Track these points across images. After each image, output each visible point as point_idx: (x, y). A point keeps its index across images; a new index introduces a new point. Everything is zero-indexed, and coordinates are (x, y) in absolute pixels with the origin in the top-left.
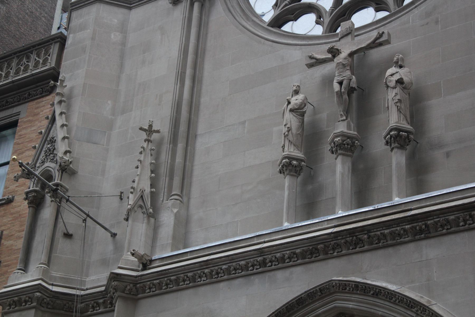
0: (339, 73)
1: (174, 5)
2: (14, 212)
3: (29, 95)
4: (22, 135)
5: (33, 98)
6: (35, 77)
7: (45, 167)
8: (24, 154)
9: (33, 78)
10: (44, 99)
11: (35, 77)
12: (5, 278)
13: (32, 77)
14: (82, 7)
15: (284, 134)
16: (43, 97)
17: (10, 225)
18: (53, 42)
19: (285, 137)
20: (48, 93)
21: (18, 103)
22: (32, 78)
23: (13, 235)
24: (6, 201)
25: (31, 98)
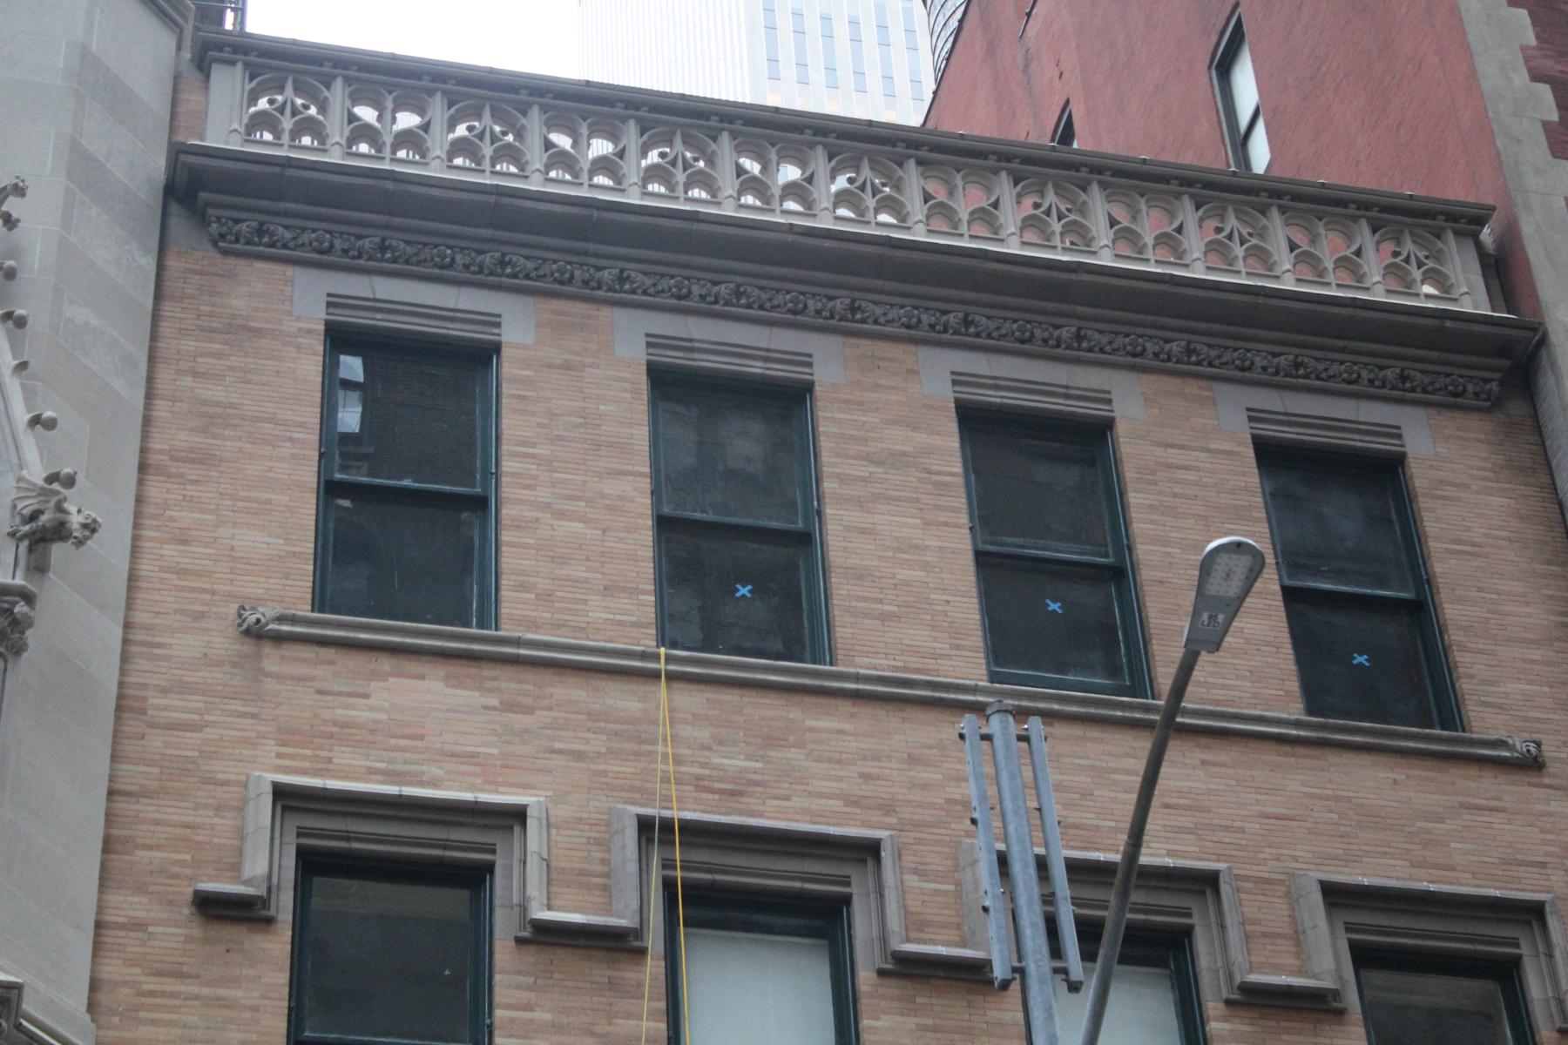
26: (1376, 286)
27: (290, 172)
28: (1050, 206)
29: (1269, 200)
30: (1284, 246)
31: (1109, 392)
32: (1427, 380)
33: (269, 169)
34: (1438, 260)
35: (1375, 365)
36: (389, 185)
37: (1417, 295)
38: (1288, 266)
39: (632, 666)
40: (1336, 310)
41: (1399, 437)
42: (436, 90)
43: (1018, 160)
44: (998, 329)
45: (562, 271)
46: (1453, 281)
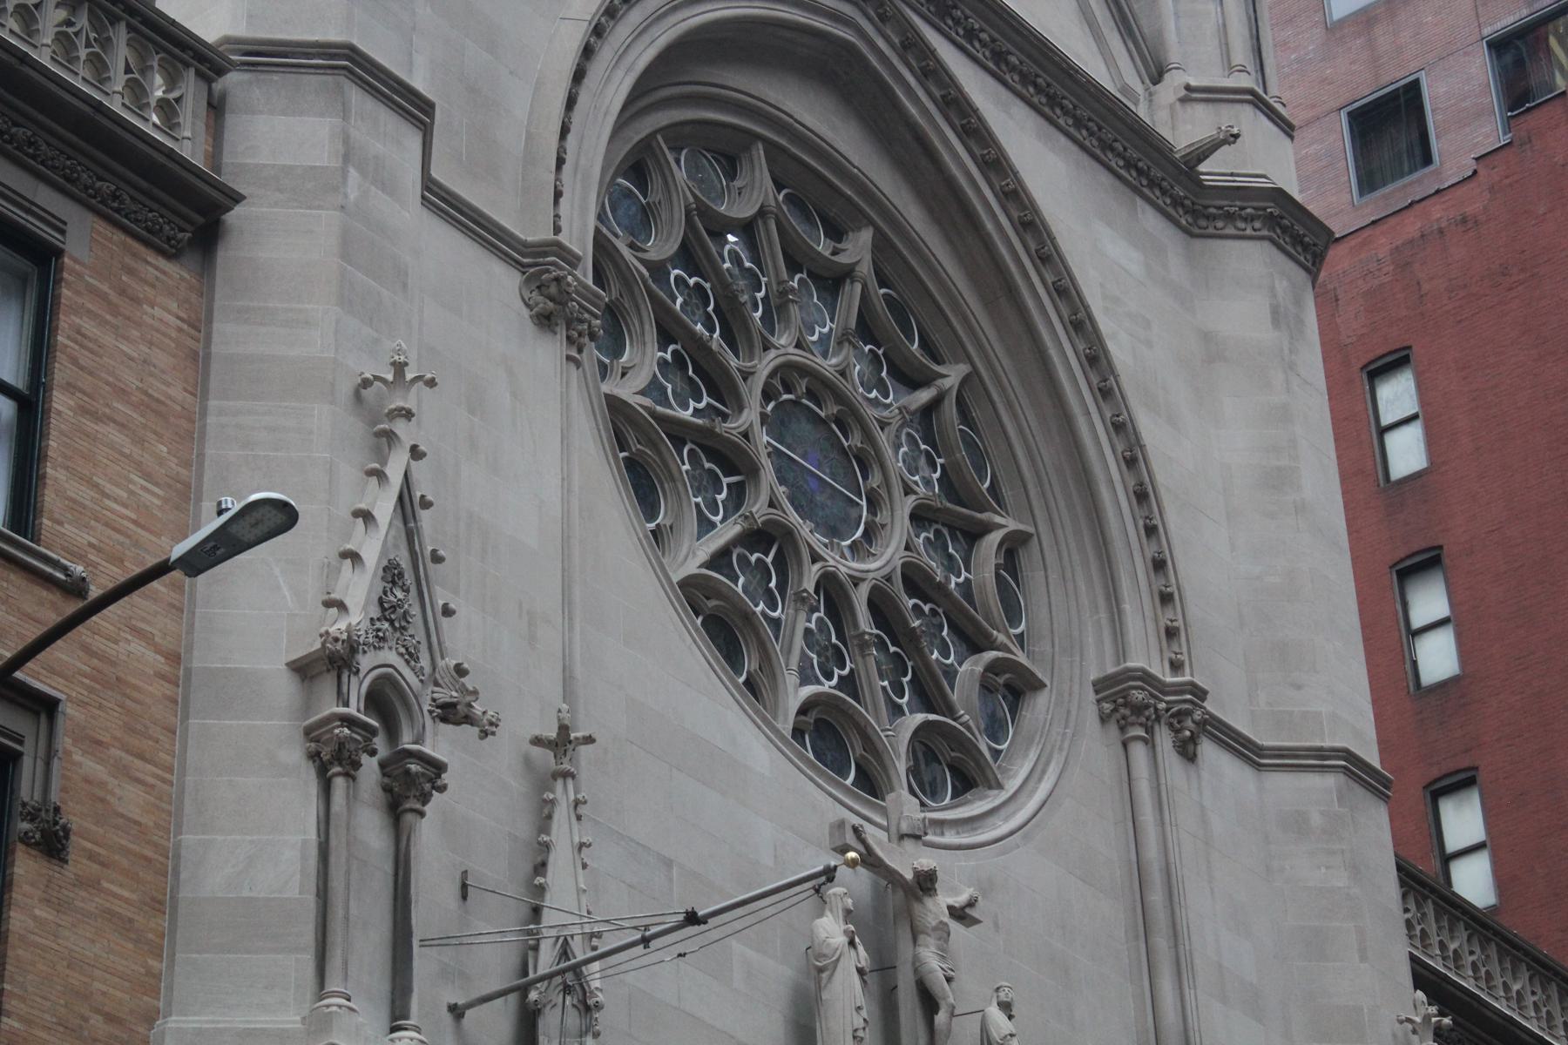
0: (939, 949)
1: (537, 322)
2: (94, 649)
3: (115, 197)
4: (84, 336)
5: (117, 216)
6: (171, 165)
7: (387, 662)
8: (100, 428)
9: (163, 166)
10: (151, 257)
11: (171, 165)
12: (94, 905)
13: (165, 158)
14: (378, 95)
15: (856, 1030)
16: (147, 243)
17: (86, 693)
18: (195, 63)
19: (854, 1037)
20: (174, 251)
21: (61, 180)
22: (161, 159)
23: (102, 742)
24: (72, 584)
25: (27, 155)
26: (185, 141)
27: (1444, 984)
28: (82, 28)
29: (191, 60)
30: (121, 66)
31: (65, 223)
32: (134, 207)
33: (1432, 977)
34: (103, 47)
35: (177, 225)
36: (1475, 1004)
37: (147, 120)
38: (120, 89)
39: (39, 568)
40: (68, 97)
41: (63, 232)
42: (192, 65)
43: (140, 19)
44: (53, 159)
45: (73, 170)
46: (40, 27)
